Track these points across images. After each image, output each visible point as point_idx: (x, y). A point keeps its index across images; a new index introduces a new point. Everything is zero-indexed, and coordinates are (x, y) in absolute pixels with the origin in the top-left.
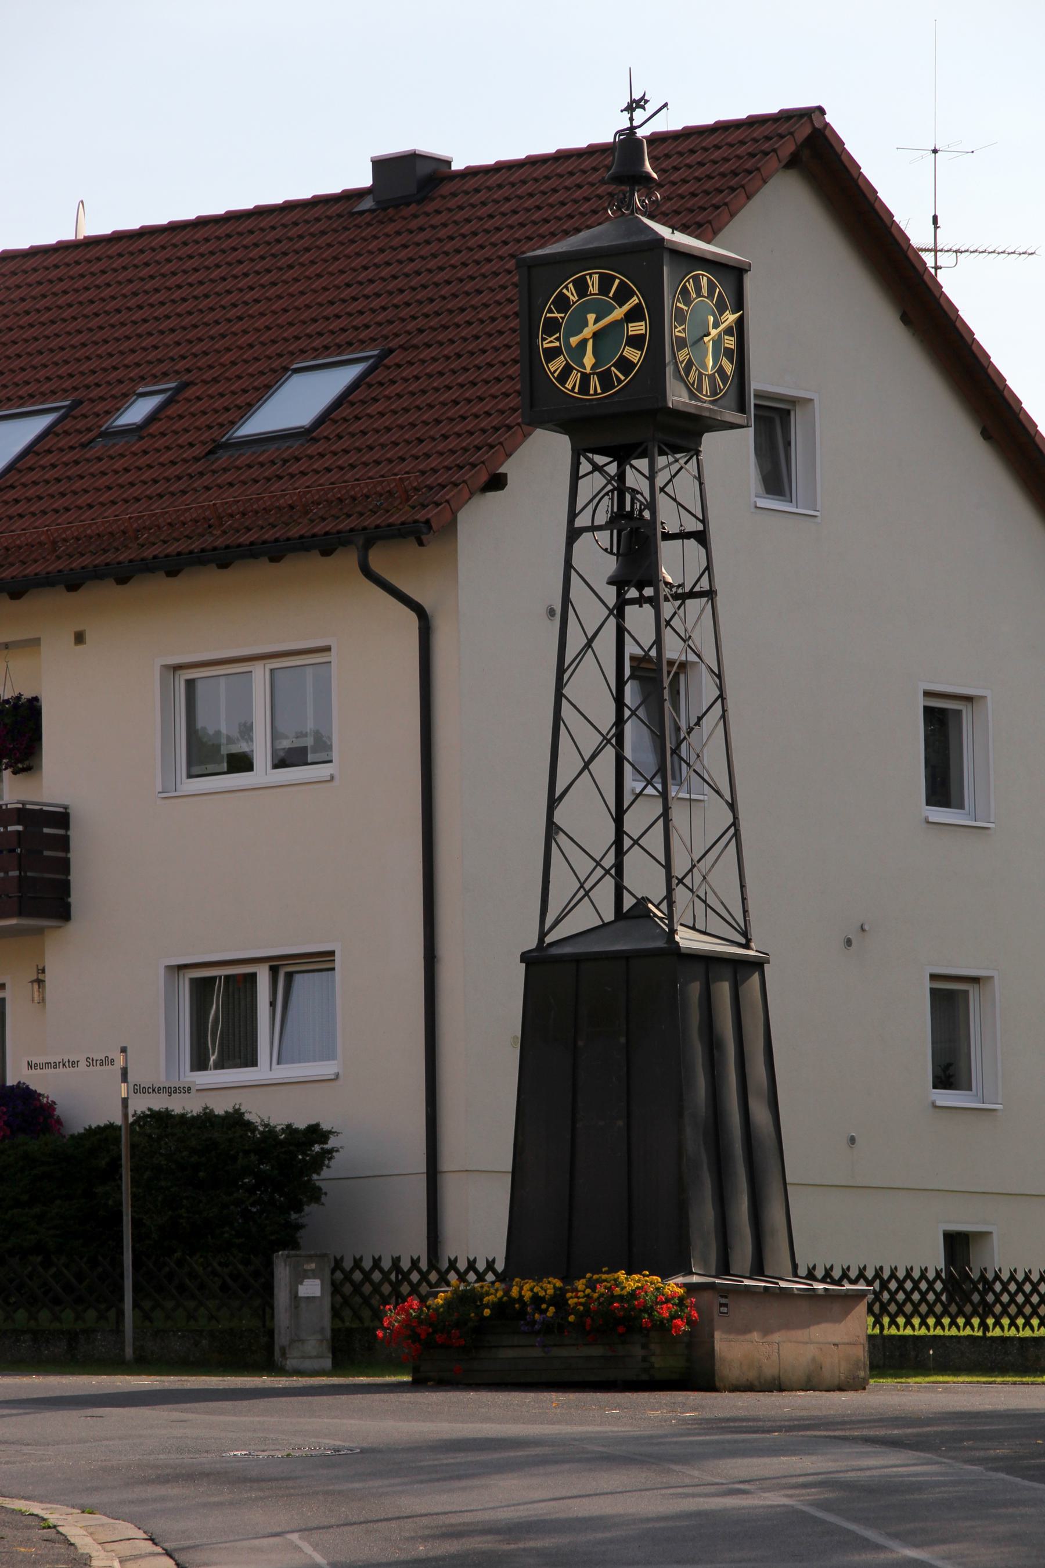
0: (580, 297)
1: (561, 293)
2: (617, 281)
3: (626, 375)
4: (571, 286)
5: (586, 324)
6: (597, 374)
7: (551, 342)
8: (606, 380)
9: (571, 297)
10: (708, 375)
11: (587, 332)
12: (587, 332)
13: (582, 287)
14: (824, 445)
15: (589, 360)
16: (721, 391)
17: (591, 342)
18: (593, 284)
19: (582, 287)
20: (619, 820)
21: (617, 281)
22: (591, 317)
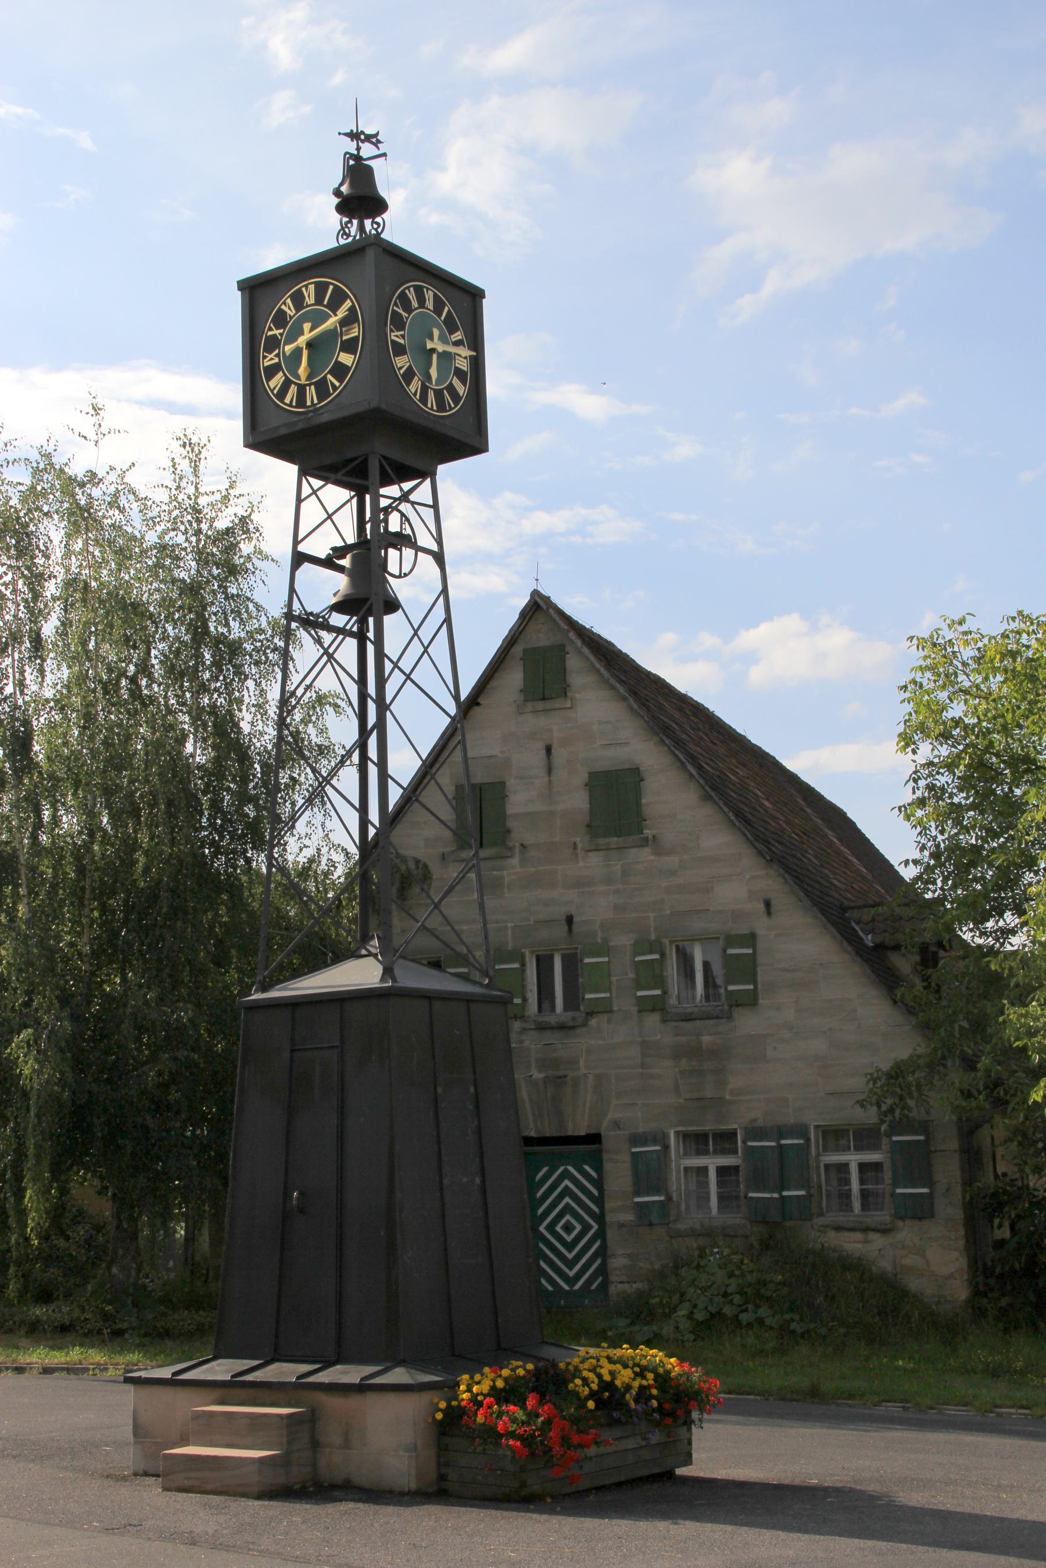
0: (298, 310)
1: (280, 309)
2: (331, 287)
3: (341, 381)
4: (289, 301)
5: (301, 333)
6: (314, 384)
7: (272, 359)
8: (322, 389)
9: (289, 312)
10: (435, 391)
11: (302, 341)
12: (302, 341)
13: (298, 300)
14: (858, 1109)
15: (303, 370)
16: (396, 304)
17: (305, 353)
18: (310, 295)
19: (298, 300)
20: (444, 916)
21: (331, 287)
22: (307, 326)
